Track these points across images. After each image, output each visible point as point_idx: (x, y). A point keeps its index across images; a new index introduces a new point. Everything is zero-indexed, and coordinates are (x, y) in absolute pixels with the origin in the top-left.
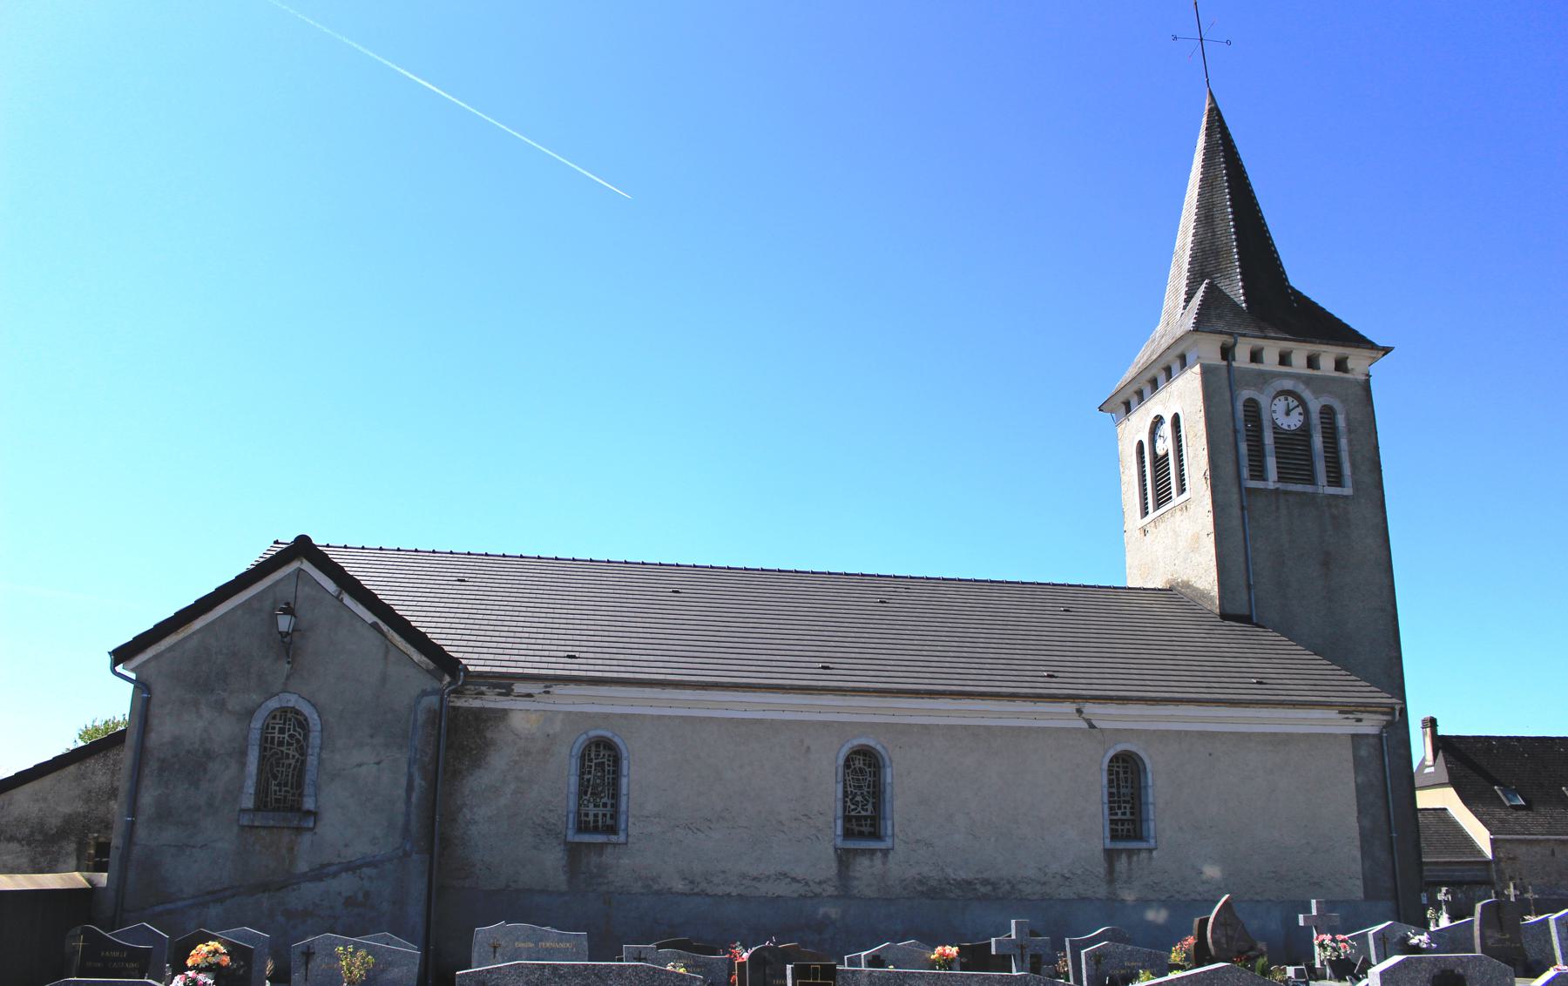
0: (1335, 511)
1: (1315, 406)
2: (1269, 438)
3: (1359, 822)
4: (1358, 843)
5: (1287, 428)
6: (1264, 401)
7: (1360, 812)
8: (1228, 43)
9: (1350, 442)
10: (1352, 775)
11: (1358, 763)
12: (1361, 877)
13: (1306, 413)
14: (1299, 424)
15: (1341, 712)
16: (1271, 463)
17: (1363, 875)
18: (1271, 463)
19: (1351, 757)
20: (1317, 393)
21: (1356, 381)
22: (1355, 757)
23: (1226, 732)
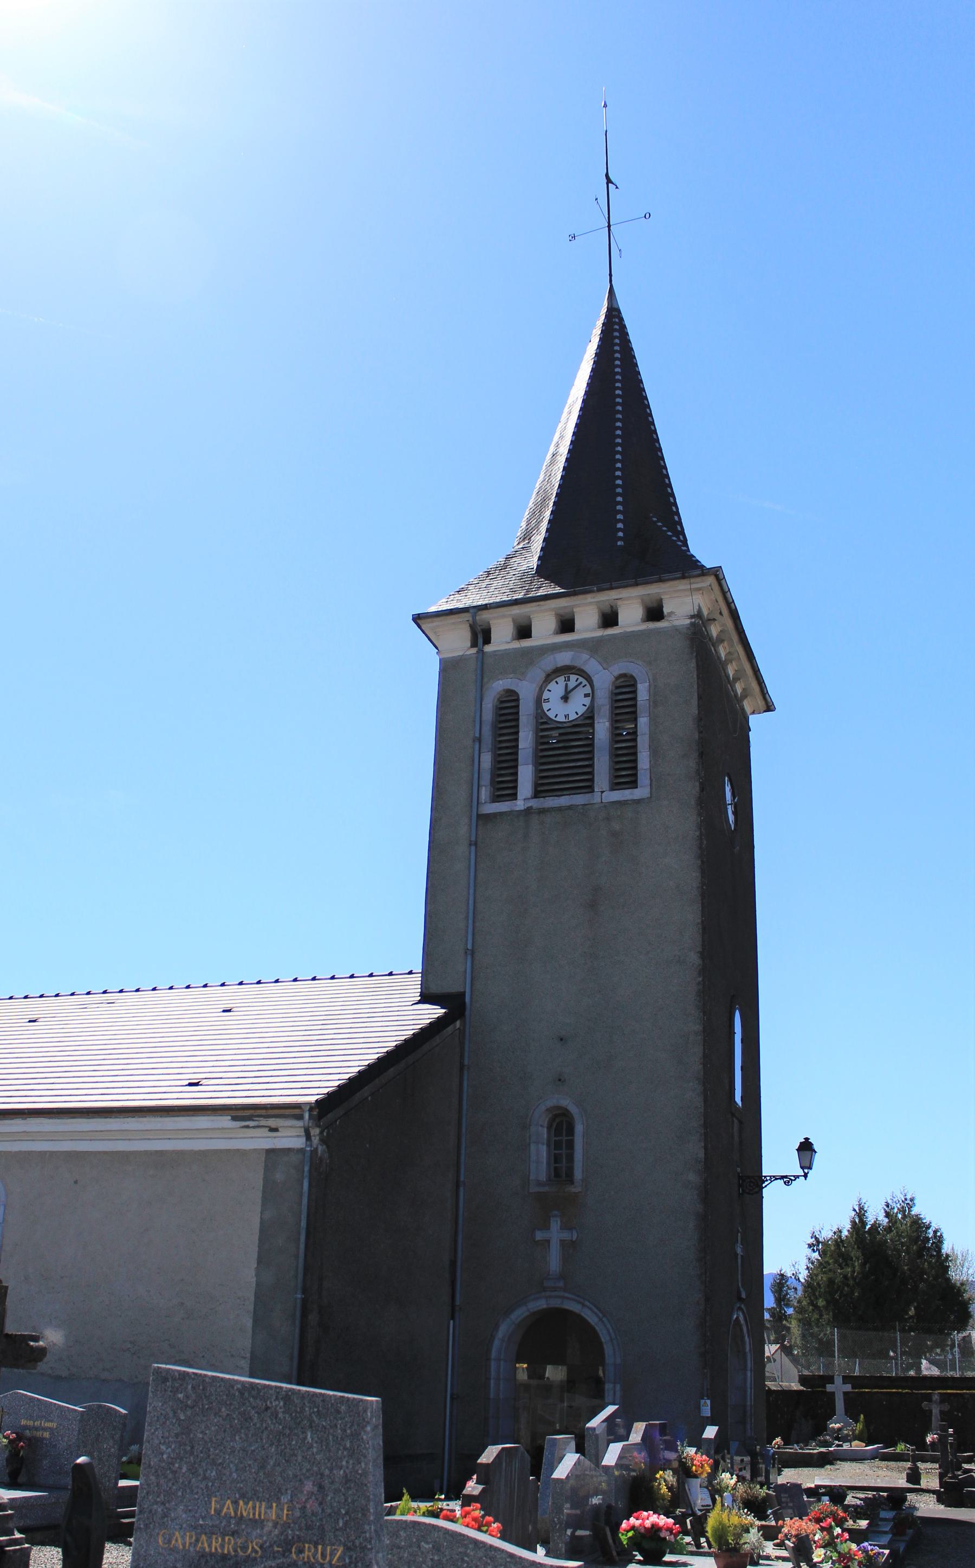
0: (616, 826)
1: (604, 679)
2: (526, 740)
3: (257, 1275)
4: (251, 1308)
5: (563, 720)
6: (526, 691)
7: (259, 1261)
8: (596, 199)
9: (653, 720)
10: (258, 1208)
11: (270, 1192)
12: (248, 1355)
13: (592, 695)
14: (551, 715)
15: (234, 1119)
16: (526, 775)
17: (252, 1353)
18: (526, 775)
19: (260, 1184)
20: (606, 662)
21: (676, 629)
22: (266, 1180)
23: (99, 1152)
